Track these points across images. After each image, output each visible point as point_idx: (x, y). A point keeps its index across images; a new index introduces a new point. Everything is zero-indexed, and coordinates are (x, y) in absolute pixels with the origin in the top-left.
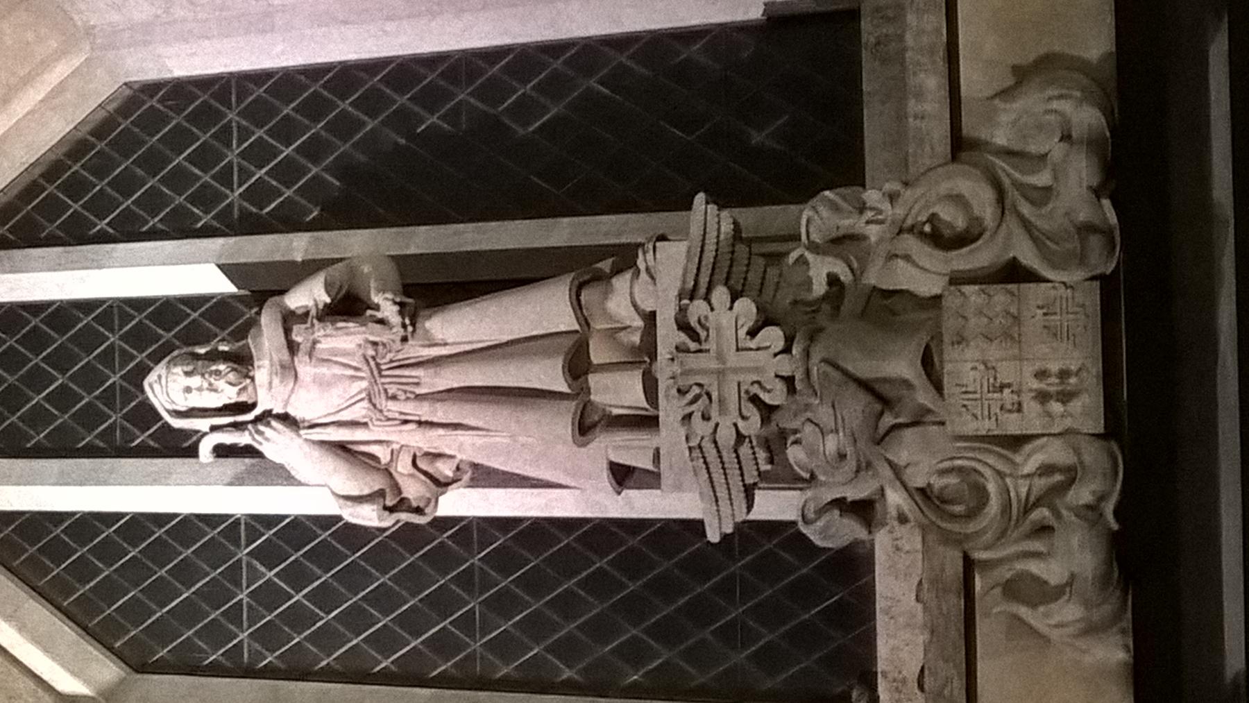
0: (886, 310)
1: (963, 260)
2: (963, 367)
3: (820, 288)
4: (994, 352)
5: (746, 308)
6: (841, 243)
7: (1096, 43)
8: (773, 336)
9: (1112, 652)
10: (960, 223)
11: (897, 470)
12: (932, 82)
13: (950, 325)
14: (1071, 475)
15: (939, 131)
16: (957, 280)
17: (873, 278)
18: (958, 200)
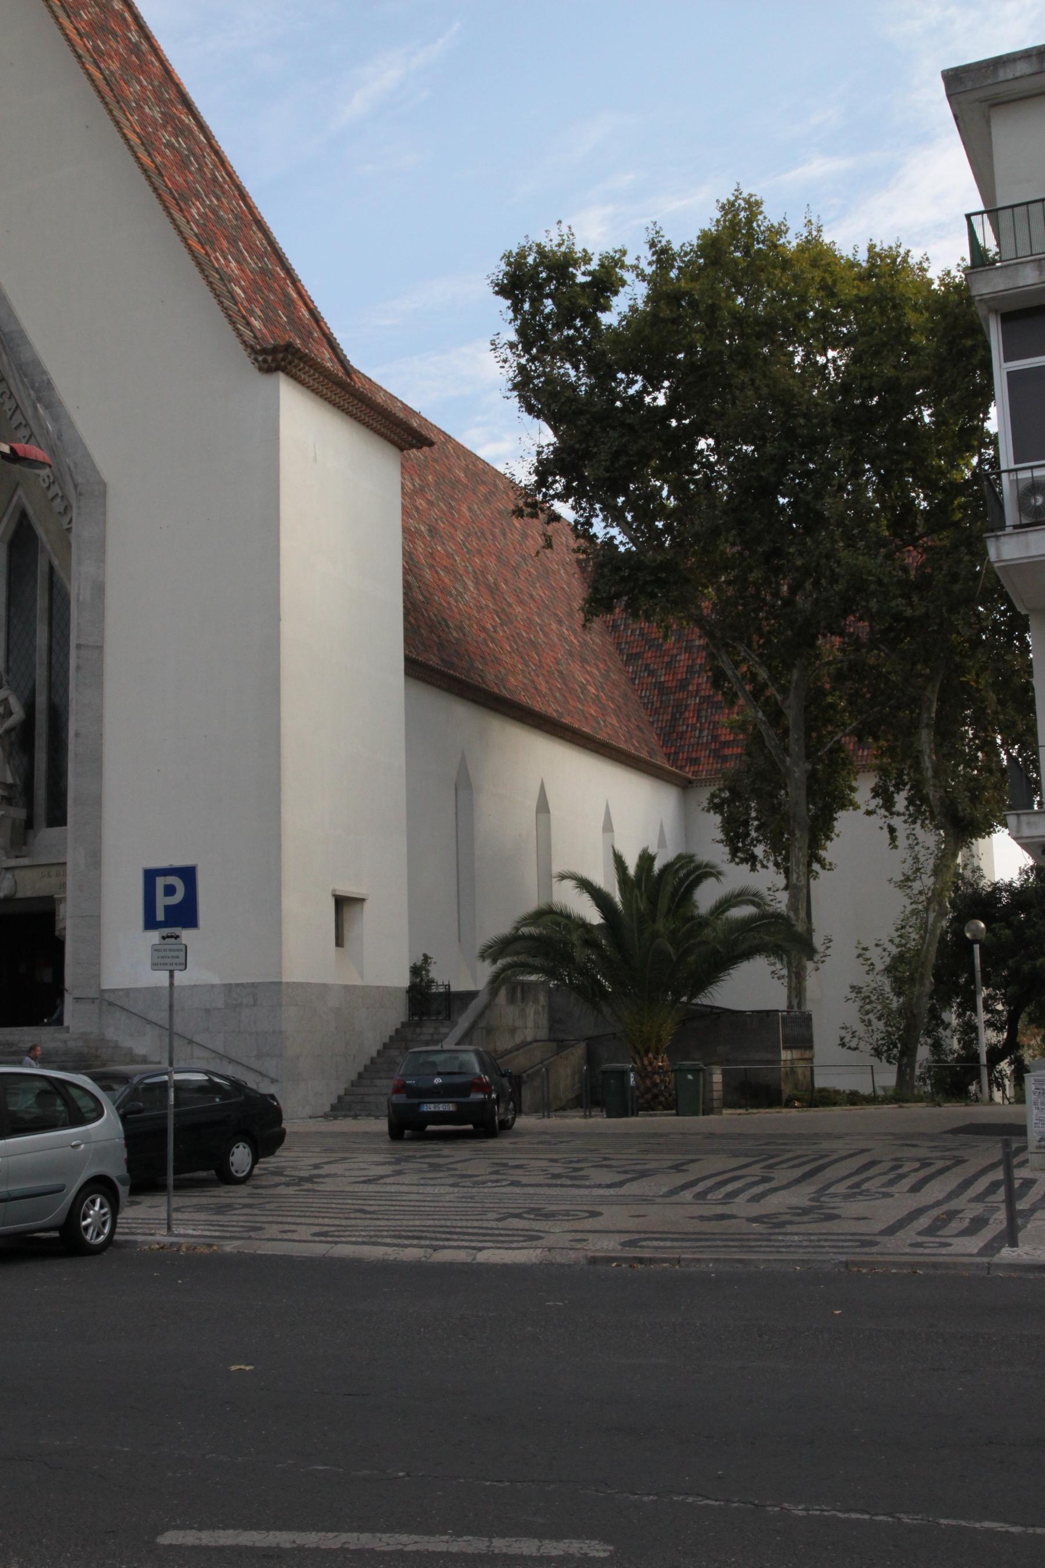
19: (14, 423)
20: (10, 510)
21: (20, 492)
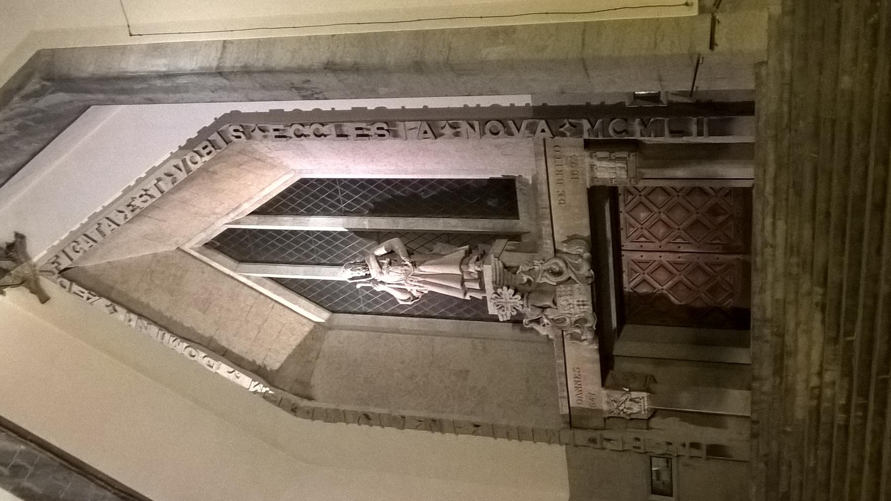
0: (541, 290)
1: (560, 279)
2: (561, 301)
3: (525, 280)
4: (568, 297)
5: (511, 291)
6: (529, 272)
7: (586, 233)
8: (518, 296)
9: (595, 347)
10: (558, 269)
11: (546, 316)
12: (549, 242)
13: (558, 294)
14: (585, 321)
15: (552, 251)
16: (559, 284)
17: (539, 280)
18: (556, 264)
19: (96, 236)
20: (205, 259)
21: (186, 248)
